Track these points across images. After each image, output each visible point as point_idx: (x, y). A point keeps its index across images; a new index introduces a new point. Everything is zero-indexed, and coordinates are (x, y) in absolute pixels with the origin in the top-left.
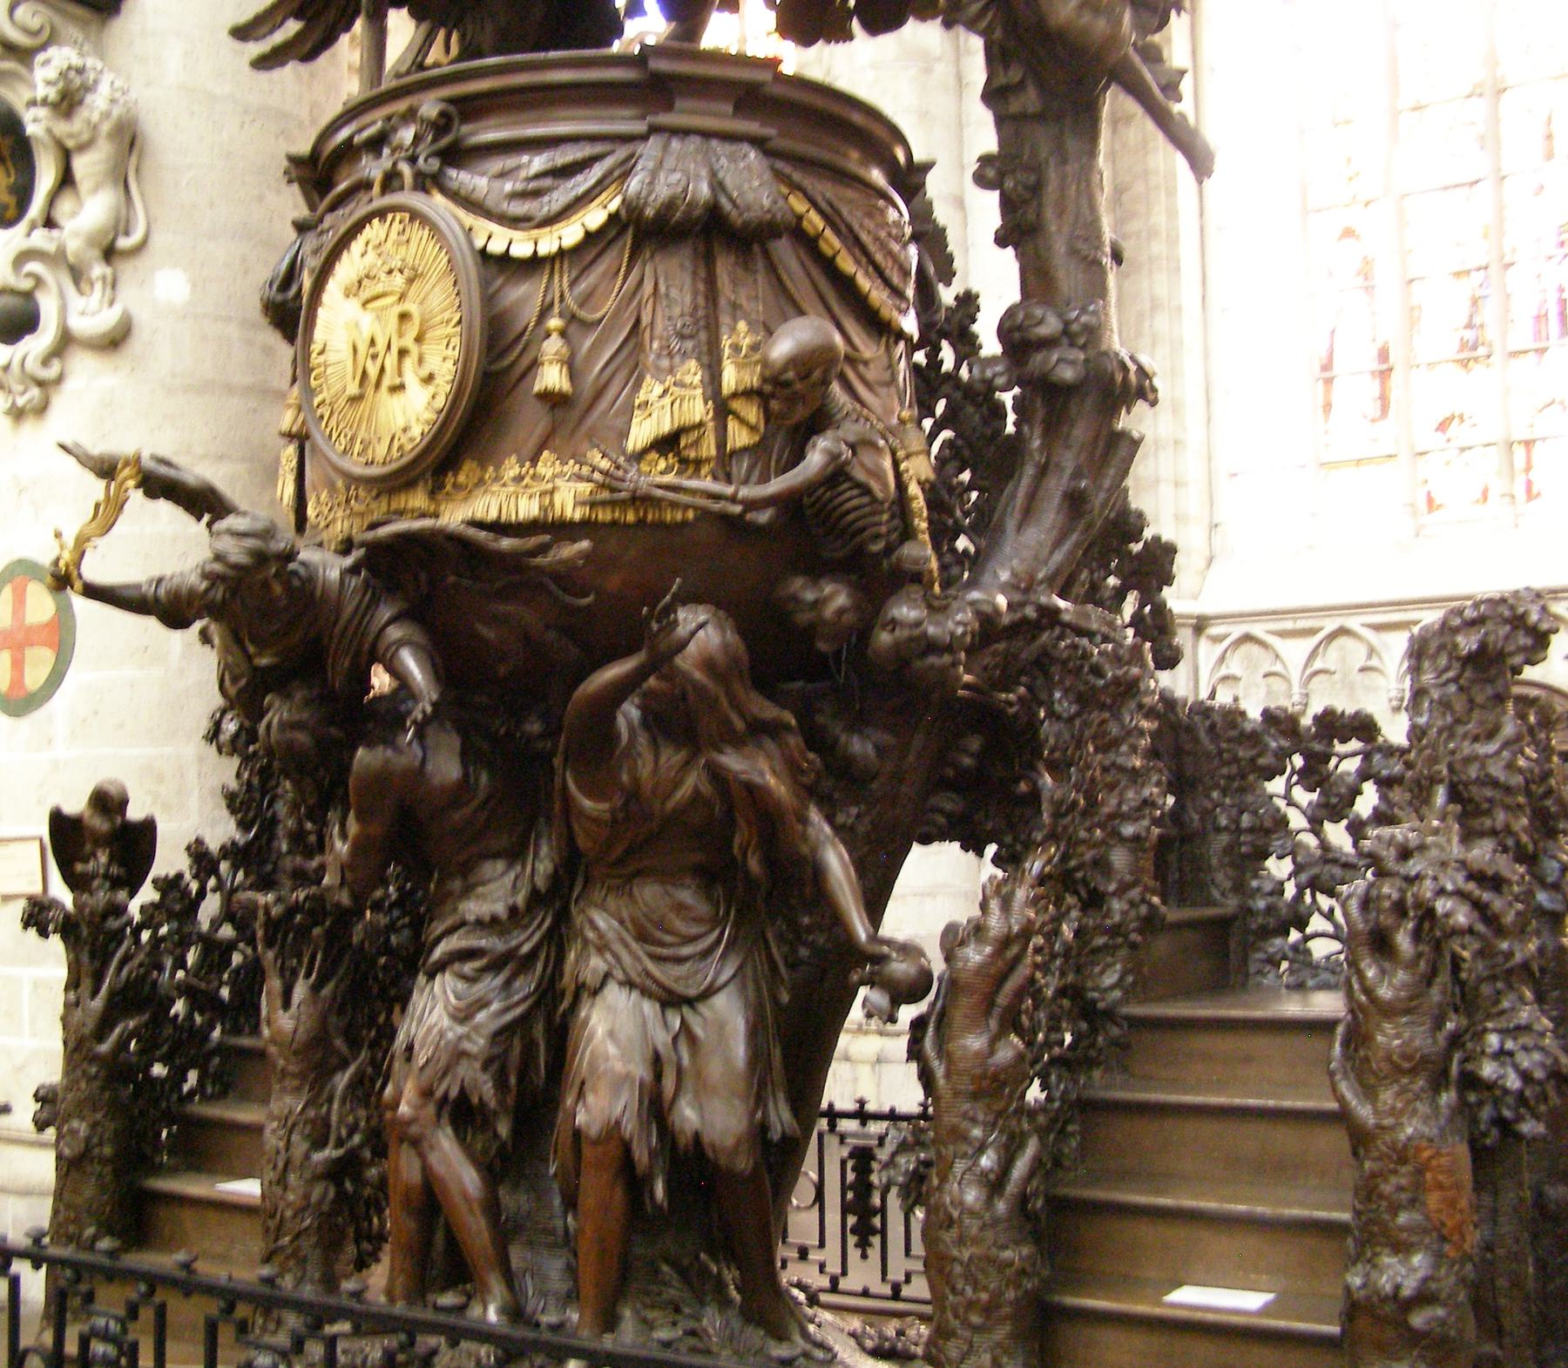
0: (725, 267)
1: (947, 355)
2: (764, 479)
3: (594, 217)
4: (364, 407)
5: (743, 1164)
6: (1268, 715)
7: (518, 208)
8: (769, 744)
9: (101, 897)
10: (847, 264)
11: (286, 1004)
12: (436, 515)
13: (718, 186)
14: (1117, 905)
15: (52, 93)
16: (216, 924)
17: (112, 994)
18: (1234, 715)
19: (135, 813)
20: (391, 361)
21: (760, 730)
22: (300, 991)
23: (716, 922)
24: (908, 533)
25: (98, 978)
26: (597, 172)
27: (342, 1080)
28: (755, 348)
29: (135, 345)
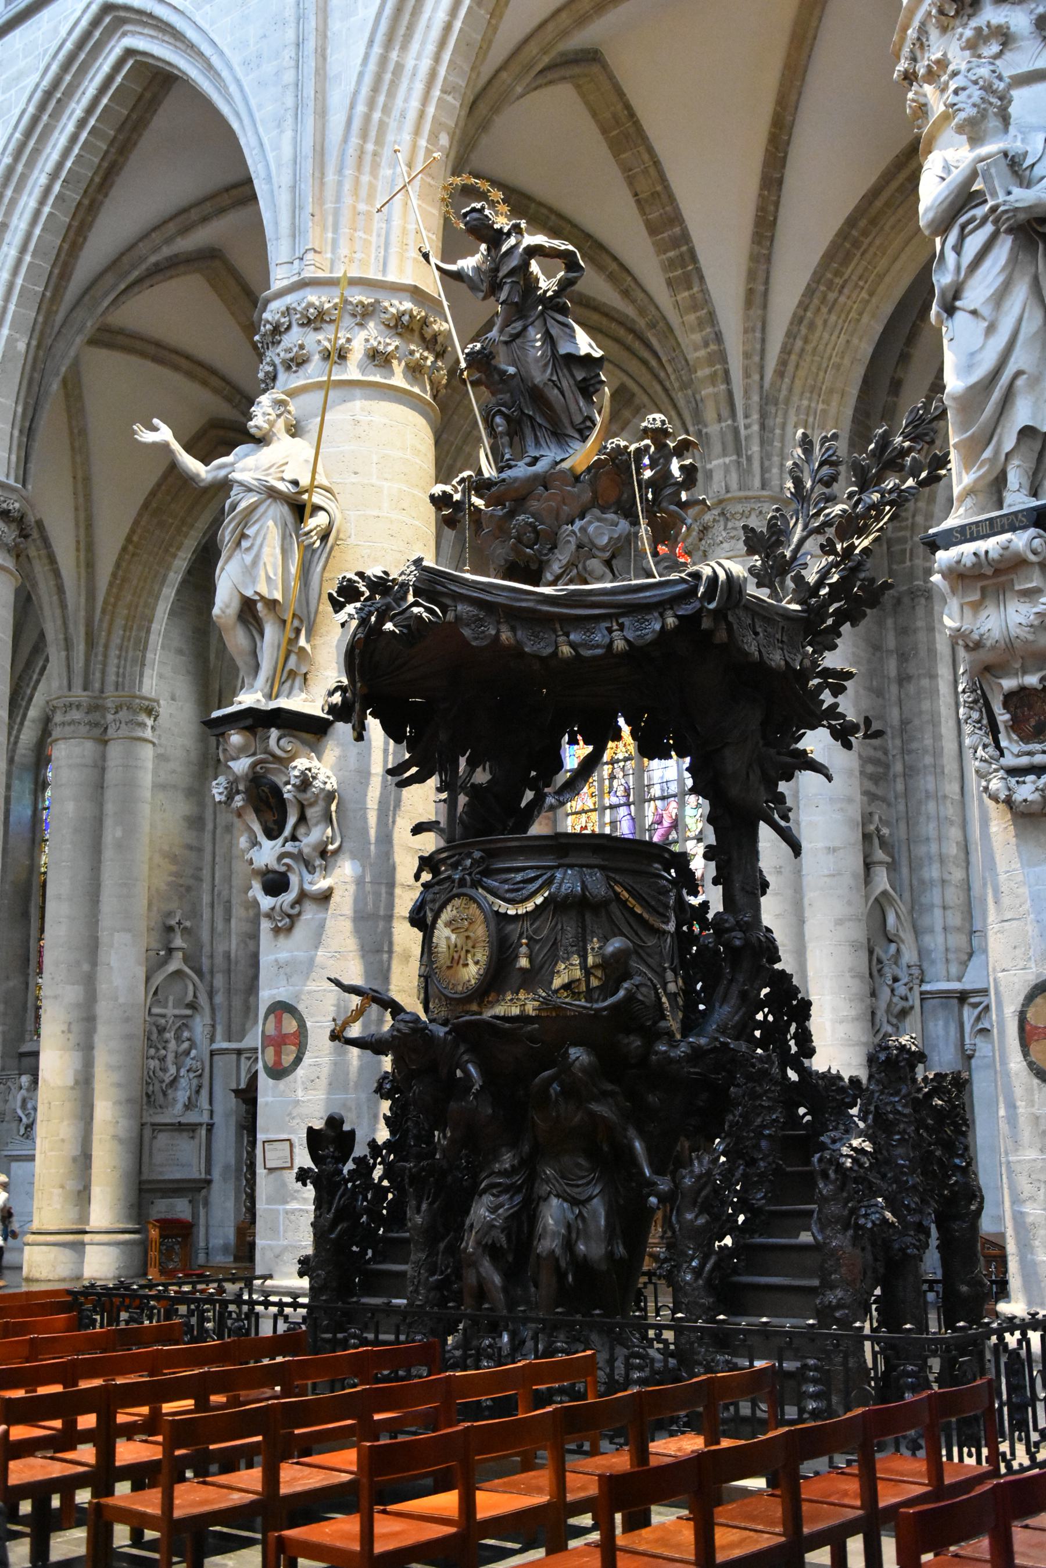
0: (588, 917)
1: (696, 928)
2: (604, 1000)
3: (539, 900)
4: (452, 971)
5: (604, 1267)
6: (851, 1079)
7: (508, 895)
8: (610, 1100)
9: (330, 1167)
10: (639, 910)
11: (418, 1211)
12: (480, 1013)
13: (584, 887)
14: (762, 1164)
15: (298, 782)
16: (381, 1179)
17: (337, 1210)
18: (839, 1077)
19: (346, 1127)
20: (463, 954)
21: (605, 1094)
22: (424, 1206)
23: (593, 1170)
24: (663, 1017)
25: (331, 1204)
26: (540, 881)
27: (442, 1246)
28: (600, 948)
29: (335, 899)
